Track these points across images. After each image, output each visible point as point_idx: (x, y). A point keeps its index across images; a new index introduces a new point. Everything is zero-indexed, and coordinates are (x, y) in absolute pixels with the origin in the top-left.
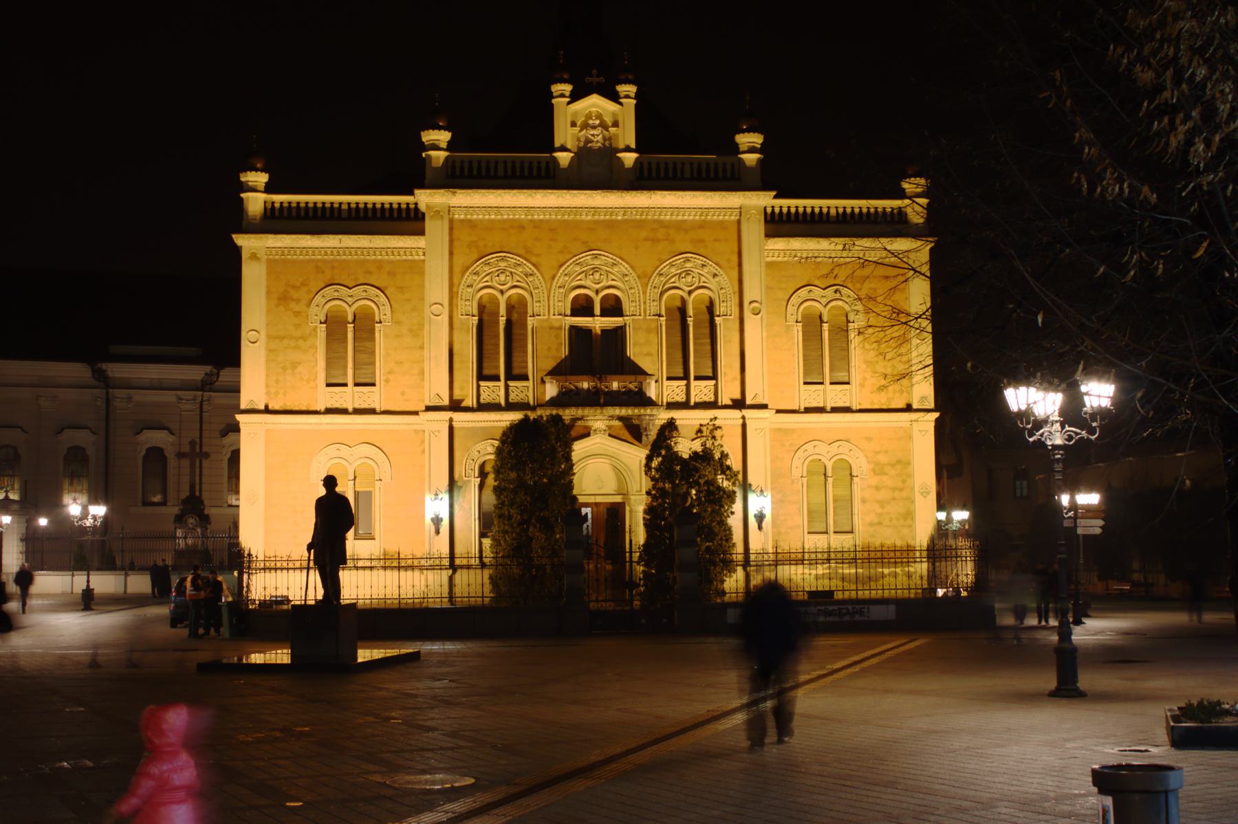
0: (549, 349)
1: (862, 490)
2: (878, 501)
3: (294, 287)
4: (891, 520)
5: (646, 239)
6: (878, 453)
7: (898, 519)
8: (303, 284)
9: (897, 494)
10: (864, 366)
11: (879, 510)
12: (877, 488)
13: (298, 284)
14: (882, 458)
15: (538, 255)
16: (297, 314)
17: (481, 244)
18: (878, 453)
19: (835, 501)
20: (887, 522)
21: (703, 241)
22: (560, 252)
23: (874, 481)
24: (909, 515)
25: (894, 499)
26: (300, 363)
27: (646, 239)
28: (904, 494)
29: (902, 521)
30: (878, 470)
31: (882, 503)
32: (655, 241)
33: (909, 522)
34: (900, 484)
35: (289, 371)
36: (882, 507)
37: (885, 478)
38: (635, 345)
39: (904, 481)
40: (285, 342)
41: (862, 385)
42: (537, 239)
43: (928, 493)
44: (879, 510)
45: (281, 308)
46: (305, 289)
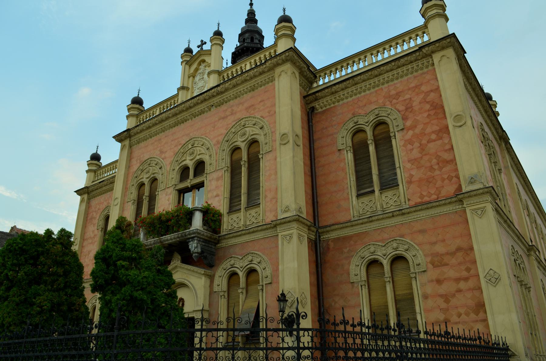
1: (423, 285)
2: (441, 296)
4: (459, 315)
7: (467, 314)
9: (462, 285)
10: (409, 165)
11: (444, 305)
12: (439, 282)
14: (440, 248)
18: (435, 243)
19: (396, 301)
20: (454, 318)
21: (253, 105)
23: (433, 274)
24: (480, 307)
25: (459, 291)
28: (471, 283)
29: (473, 316)
30: (438, 261)
31: (446, 298)
33: (481, 316)
34: (465, 274)
36: (447, 301)
37: (445, 269)
39: (468, 270)
41: (410, 182)
43: (498, 279)
44: (444, 305)
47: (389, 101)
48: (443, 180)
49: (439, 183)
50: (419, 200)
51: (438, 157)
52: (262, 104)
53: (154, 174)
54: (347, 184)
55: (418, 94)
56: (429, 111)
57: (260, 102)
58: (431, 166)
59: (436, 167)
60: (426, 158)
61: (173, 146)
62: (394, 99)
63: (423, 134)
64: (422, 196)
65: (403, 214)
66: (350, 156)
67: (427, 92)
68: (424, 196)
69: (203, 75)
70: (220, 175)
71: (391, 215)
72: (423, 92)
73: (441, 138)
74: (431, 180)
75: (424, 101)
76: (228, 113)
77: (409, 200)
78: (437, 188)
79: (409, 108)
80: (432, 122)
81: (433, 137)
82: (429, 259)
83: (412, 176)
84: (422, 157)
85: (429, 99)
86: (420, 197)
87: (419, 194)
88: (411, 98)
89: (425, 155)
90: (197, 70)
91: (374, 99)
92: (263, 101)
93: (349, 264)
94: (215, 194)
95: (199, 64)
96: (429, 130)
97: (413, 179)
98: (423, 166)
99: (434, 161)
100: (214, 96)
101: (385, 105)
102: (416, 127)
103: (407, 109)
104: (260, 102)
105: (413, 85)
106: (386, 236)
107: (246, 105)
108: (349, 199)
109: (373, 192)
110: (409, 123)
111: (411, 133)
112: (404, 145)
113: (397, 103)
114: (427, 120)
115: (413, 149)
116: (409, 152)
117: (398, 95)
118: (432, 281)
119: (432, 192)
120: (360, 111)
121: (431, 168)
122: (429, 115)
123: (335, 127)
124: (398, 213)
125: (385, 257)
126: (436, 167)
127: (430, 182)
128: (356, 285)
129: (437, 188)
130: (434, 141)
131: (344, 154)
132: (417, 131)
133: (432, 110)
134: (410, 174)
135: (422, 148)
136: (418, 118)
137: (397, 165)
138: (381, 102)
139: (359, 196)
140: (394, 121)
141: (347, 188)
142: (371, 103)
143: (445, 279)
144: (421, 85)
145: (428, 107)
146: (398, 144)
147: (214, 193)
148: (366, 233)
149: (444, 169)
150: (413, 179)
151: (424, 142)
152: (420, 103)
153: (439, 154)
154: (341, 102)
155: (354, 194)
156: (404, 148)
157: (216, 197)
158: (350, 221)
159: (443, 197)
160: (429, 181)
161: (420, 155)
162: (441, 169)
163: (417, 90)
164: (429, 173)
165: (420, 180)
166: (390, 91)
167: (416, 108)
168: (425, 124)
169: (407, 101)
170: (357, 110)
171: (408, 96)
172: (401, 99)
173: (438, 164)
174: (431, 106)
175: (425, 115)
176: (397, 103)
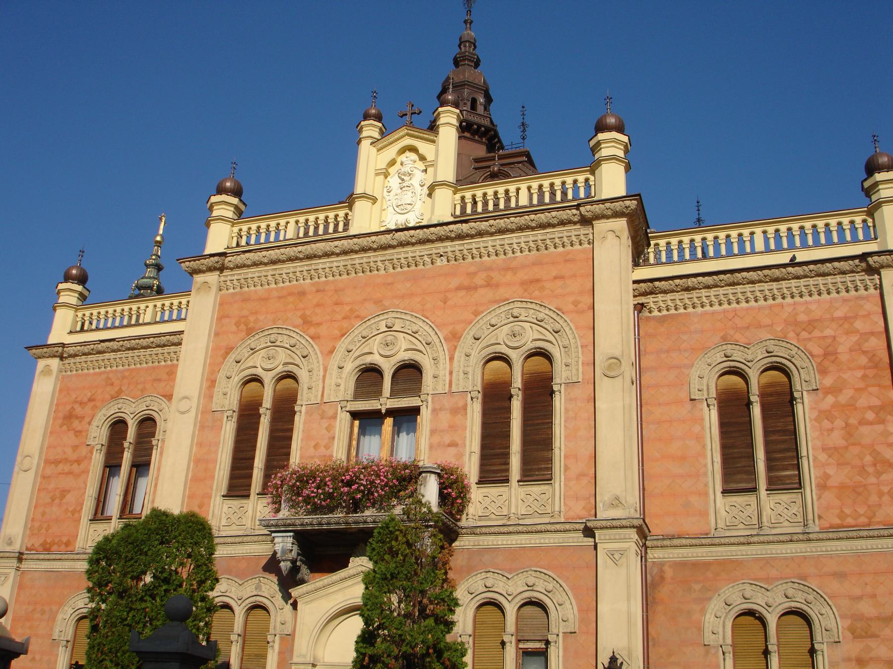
0: (316, 447)
3: (81, 403)
5: (458, 289)
6: (860, 598)
8: (90, 400)
10: (823, 457)
13: (85, 399)
14: (866, 608)
15: (319, 324)
16: (78, 433)
17: (252, 319)
18: (860, 598)
21: (538, 281)
22: (344, 318)
26: (69, 491)
27: (458, 289)
32: (471, 289)
35: (57, 501)
37: (872, 643)
38: (433, 432)
40: (61, 467)
41: (823, 487)
42: (318, 305)
45: (65, 427)
46: (91, 405)
47: (794, 331)
48: (881, 494)
49: (874, 499)
50: (837, 521)
51: (875, 453)
52: (559, 283)
53: (286, 364)
54: (705, 466)
55: (848, 333)
56: (865, 368)
57: (556, 278)
58: (863, 467)
59: (870, 470)
60: (855, 450)
61: (338, 317)
62: (804, 330)
63: (851, 406)
64: (842, 515)
65: (809, 540)
66: (712, 417)
67: (865, 334)
68: (848, 516)
70: (461, 404)
71: (787, 538)
72: (858, 331)
73: (882, 422)
74: (860, 490)
75: (857, 349)
76: (479, 280)
77: (820, 517)
78: (869, 506)
79: (830, 354)
80: (871, 389)
81: (870, 416)
82: (848, 623)
83: (827, 476)
84: (846, 448)
85: (866, 346)
86: (839, 517)
87: (837, 511)
88: (834, 338)
89: (854, 444)
90: (392, 163)
91: (767, 321)
92: (562, 278)
93: (703, 611)
94: (447, 439)
95: (402, 151)
96: (862, 402)
97: (830, 483)
98: (848, 464)
99: (868, 459)
100: (448, 238)
101: (785, 337)
102: (840, 391)
103: (826, 355)
104: (556, 278)
105: (839, 314)
106: (774, 573)
107: (522, 275)
108: (706, 494)
109: (754, 490)
110: (828, 381)
111: (830, 399)
112: (817, 419)
113: (809, 339)
114: (861, 385)
115: (832, 430)
116: (825, 433)
117: (812, 324)
118: (849, 660)
119: (861, 511)
120: (737, 336)
121: (862, 470)
122: (864, 377)
123: (686, 355)
124: (801, 537)
125: (770, 609)
126: (870, 470)
127: (859, 494)
128: (713, 651)
129: (869, 506)
130: (871, 423)
131: (702, 410)
132: (843, 398)
133: (869, 368)
134: (825, 473)
135: (849, 431)
136: (846, 376)
137: (804, 453)
138: (779, 329)
139: (725, 492)
140: (801, 370)
141: (705, 474)
142: (760, 326)
143: (871, 659)
144: (856, 317)
145: (863, 360)
146: (805, 412)
147: (445, 437)
148: (736, 564)
149: (884, 477)
150: (830, 483)
151: (853, 421)
152: (851, 350)
153: (878, 448)
154: (699, 309)
155: (719, 488)
156: (817, 425)
157: (449, 445)
158: (706, 535)
159: (878, 523)
160: (857, 491)
161: (842, 443)
162: (878, 474)
163: (846, 326)
164: (858, 478)
165: (842, 487)
166: (797, 314)
167: (844, 358)
168: (857, 390)
169: (829, 341)
170: (731, 332)
171: (828, 332)
172: (817, 333)
173: (875, 465)
174: (870, 360)
175: (859, 373)
176: (809, 339)
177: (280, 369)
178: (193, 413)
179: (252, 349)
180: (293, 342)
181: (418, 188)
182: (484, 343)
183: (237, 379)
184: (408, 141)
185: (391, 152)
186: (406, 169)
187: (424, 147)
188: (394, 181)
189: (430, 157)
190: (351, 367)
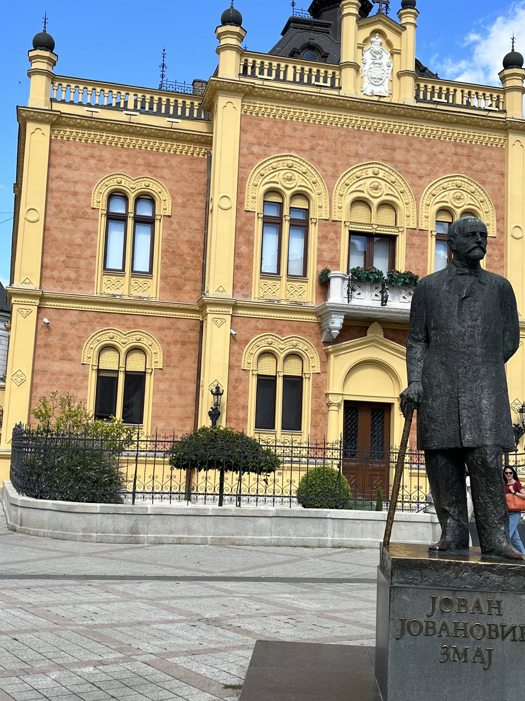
53: (300, 186)
69: (380, 58)
90: (366, 41)
177: (297, 188)
178: (234, 211)
179: (273, 169)
180: (304, 170)
181: (386, 68)
182: (437, 200)
183: (263, 189)
184: (379, 27)
185: (366, 32)
186: (378, 49)
187: (391, 35)
188: (368, 56)
189: (396, 46)
190: (350, 198)
